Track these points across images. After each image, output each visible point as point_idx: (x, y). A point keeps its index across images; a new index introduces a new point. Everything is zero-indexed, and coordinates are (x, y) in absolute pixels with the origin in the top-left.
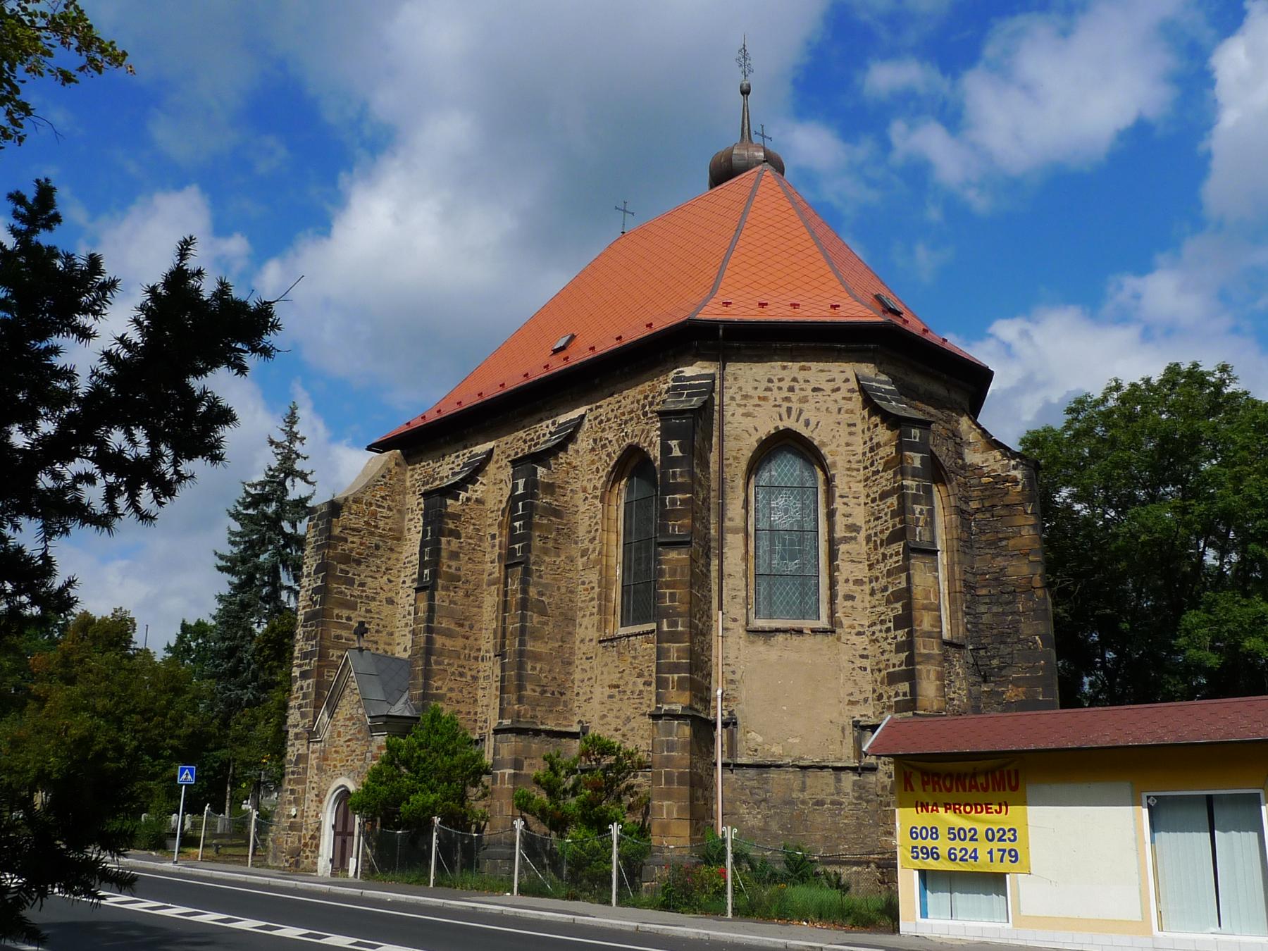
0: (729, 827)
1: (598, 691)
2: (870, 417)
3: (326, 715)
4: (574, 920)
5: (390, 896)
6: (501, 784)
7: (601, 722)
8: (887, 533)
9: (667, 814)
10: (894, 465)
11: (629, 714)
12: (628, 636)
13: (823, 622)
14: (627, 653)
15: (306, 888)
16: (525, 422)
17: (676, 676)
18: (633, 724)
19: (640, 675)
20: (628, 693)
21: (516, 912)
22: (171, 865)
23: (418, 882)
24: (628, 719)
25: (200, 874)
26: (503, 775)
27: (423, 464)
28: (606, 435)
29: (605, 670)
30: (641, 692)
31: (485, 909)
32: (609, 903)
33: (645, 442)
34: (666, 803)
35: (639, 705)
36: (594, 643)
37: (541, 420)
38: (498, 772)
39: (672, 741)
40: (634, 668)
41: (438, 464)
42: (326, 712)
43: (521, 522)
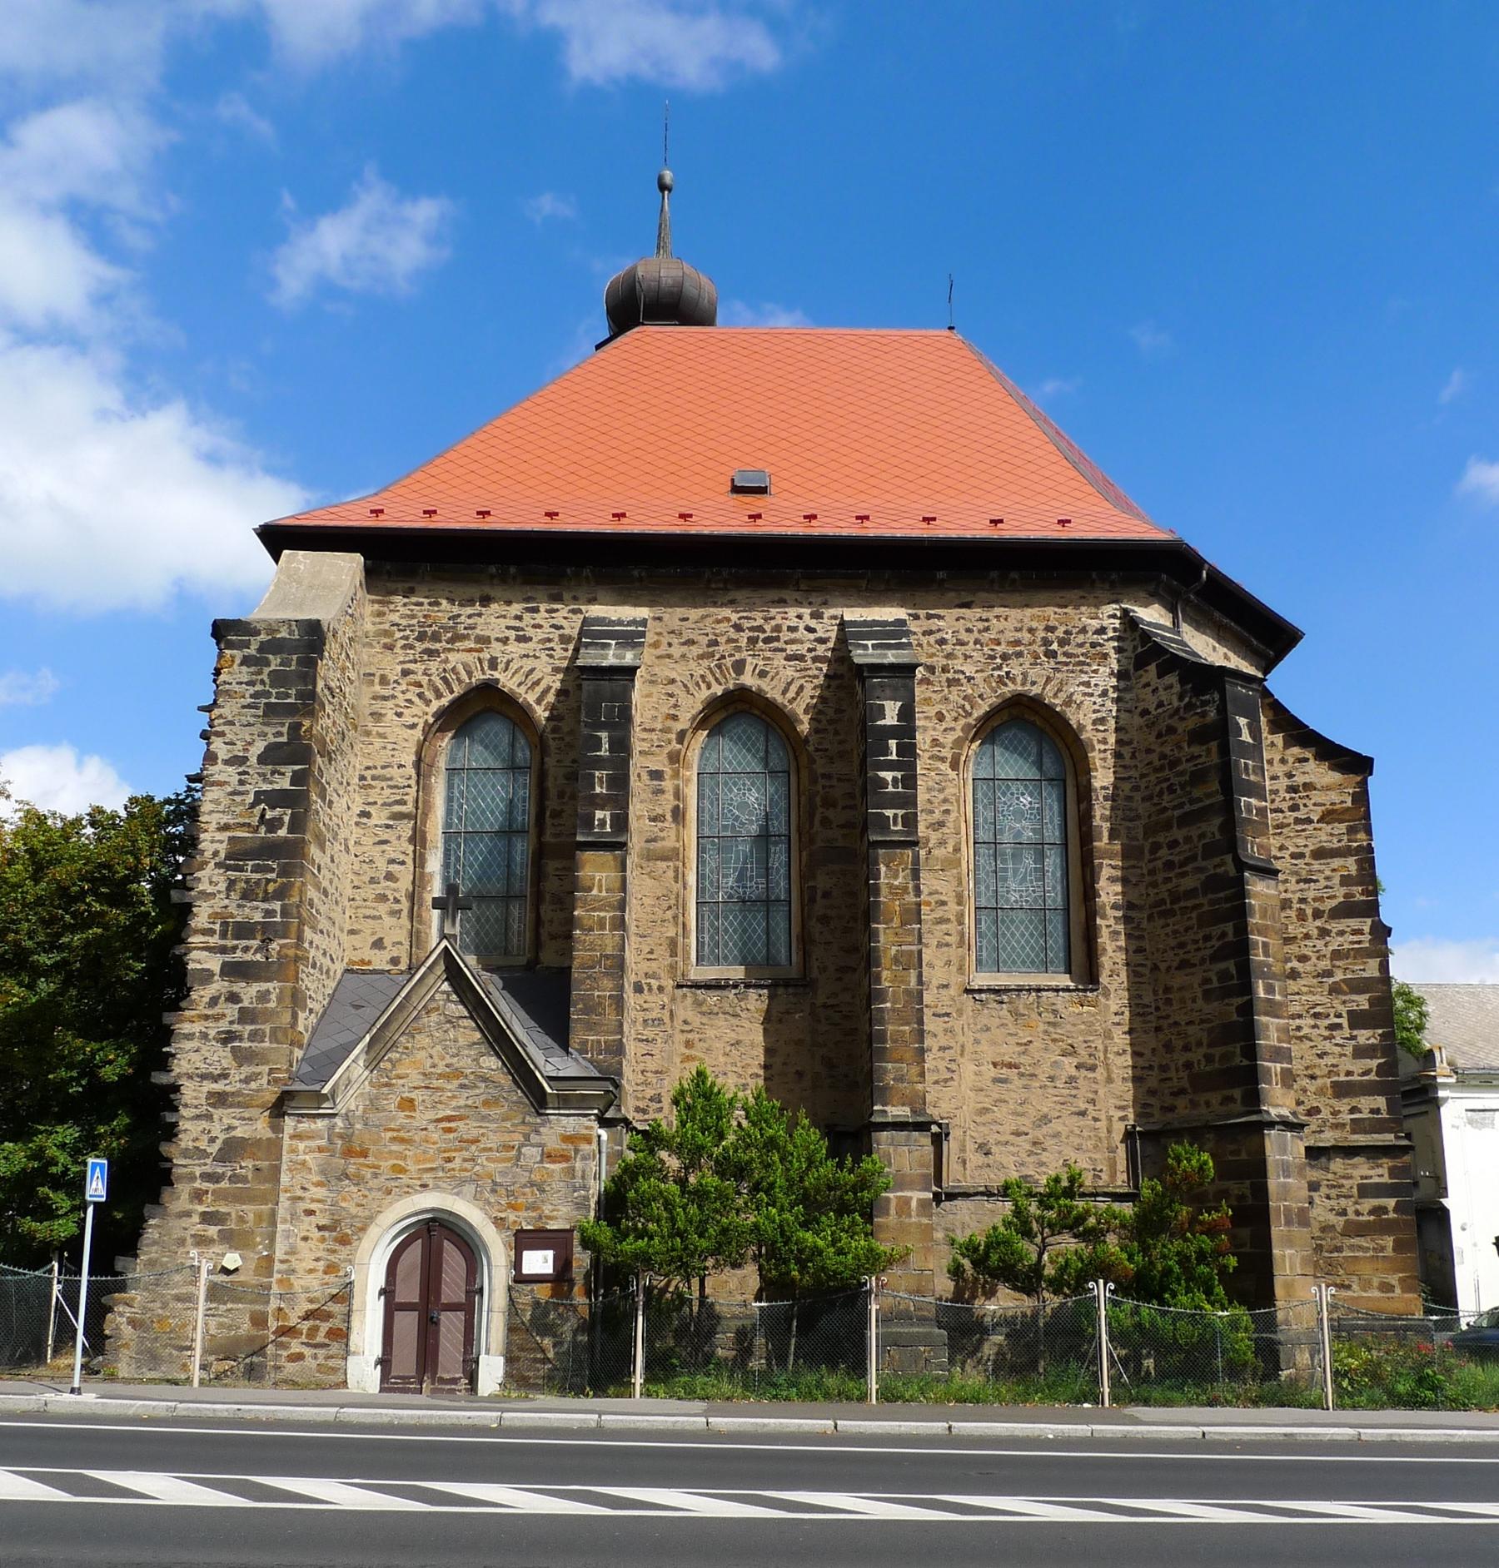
0: (1101, 1282)
1: (968, 1068)
2: (1287, 746)
3: (361, 1063)
4: (1360, 1434)
5: (1050, 1430)
6: (899, 1214)
7: (978, 1119)
8: (1334, 903)
9: (1291, 1269)
10: (1347, 818)
11: (1045, 1110)
12: (1039, 990)
13: (697, 973)
14: (1034, 1016)
15: (751, 1429)
16: (739, 595)
17: (1278, 1065)
18: (1056, 1126)
19: (1071, 1051)
20: (1043, 1077)
21: (1391, 1435)
22: (67, 1397)
23: (843, 1395)
24: (1045, 1119)
25: (1017, 1433)
26: (908, 1201)
27: (414, 599)
28: (957, 664)
29: (983, 1037)
30: (1072, 1080)
31: (1314, 1435)
32: (1097, 1399)
33: (1055, 696)
34: (1288, 1252)
35: (1071, 1099)
36: (952, 991)
37: (782, 602)
38: (891, 1195)
39: (1288, 1161)
40: (1054, 1040)
41: (469, 610)
42: (363, 1056)
43: (899, 775)
